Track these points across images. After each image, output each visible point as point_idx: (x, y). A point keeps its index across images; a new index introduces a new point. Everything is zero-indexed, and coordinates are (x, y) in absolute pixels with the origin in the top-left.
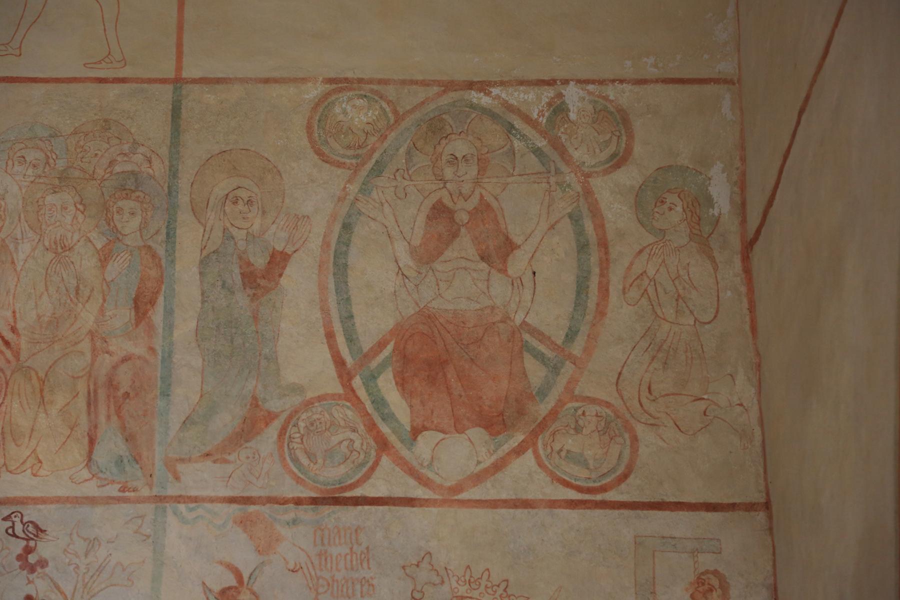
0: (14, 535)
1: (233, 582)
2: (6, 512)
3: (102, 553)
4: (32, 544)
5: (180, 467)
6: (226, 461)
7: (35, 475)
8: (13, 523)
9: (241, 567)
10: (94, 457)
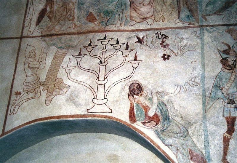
0: (159, 38)
1: (227, 48)
2: (156, 32)
3: (185, 42)
4: (164, 40)
5: (207, 18)
6: (222, 15)
7: (163, 22)
8: (158, 35)
9: (229, 44)
10: (180, 16)
